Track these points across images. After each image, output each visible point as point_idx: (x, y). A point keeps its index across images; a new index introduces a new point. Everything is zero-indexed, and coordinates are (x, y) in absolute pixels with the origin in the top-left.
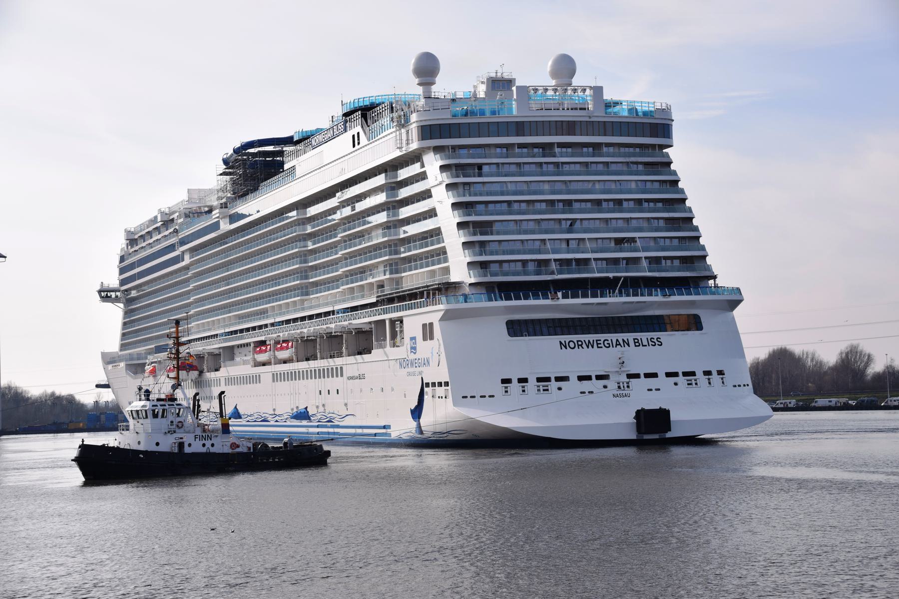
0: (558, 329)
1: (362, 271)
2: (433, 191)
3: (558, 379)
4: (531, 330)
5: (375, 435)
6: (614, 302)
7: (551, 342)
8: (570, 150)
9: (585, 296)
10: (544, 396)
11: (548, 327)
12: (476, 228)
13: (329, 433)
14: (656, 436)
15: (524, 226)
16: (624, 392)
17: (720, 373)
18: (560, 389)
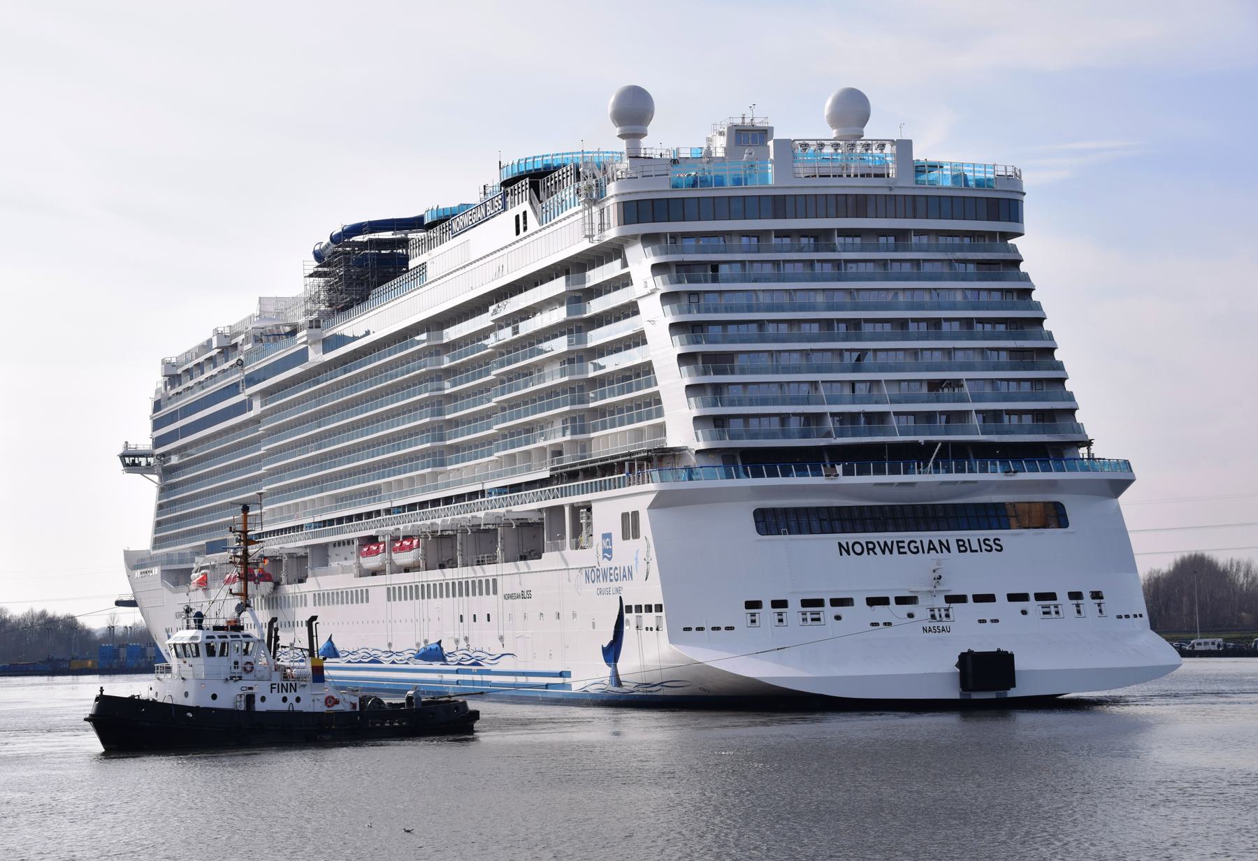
0: (837, 524)
1: (529, 429)
2: (640, 303)
3: (836, 602)
5: (547, 686)
6: (926, 482)
8: (858, 240)
9: (879, 471)
10: (813, 629)
12: (708, 362)
13: (474, 682)
14: (991, 695)
15: (784, 360)
17: (1097, 595)
18: (838, 618)
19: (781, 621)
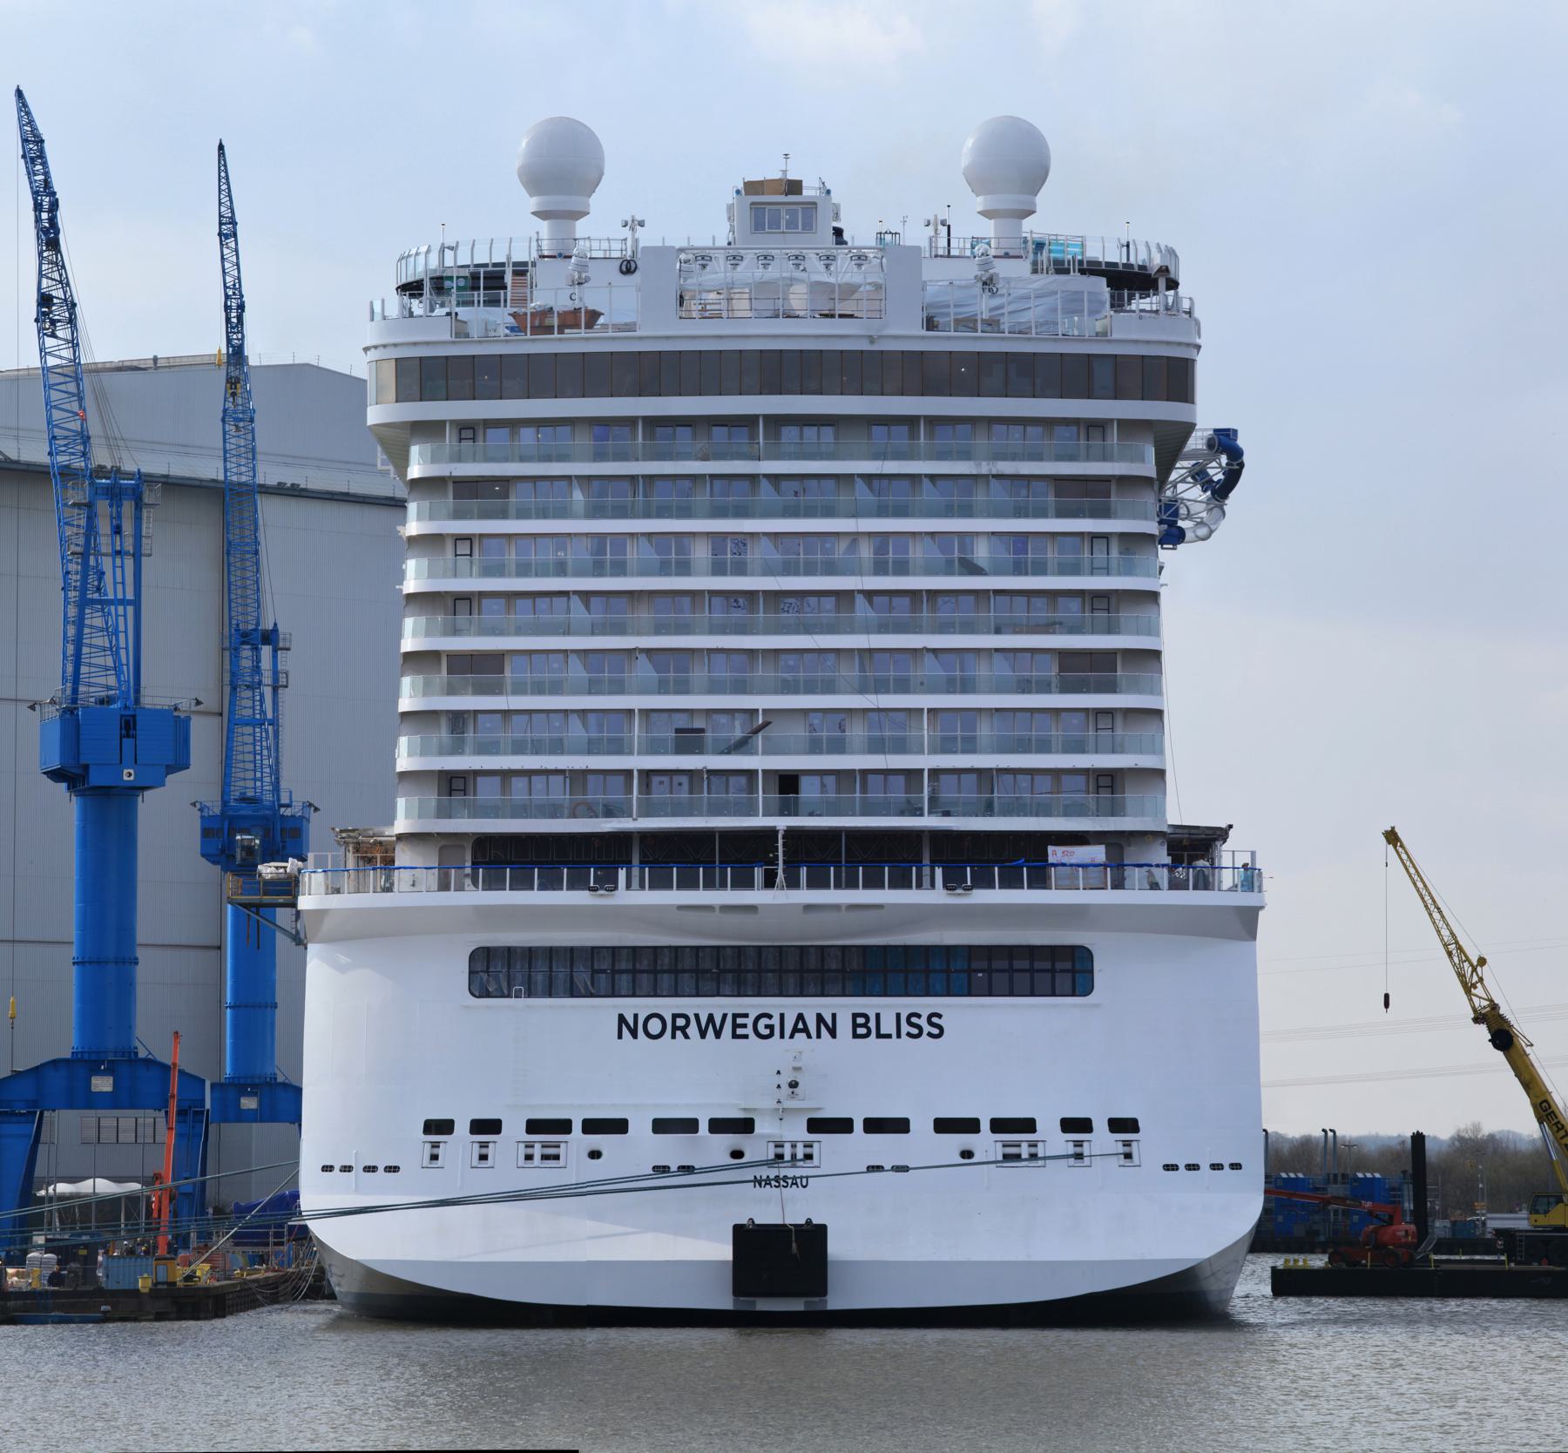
0: (687, 980)
3: (591, 1126)
4: (539, 978)
6: (780, 907)
7: (592, 1017)
9: (688, 883)
11: (594, 972)
14: (796, 1305)
16: (791, 1172)
17: (1122, 1125)
18: (595, 1155)
19: (483, 1157)
